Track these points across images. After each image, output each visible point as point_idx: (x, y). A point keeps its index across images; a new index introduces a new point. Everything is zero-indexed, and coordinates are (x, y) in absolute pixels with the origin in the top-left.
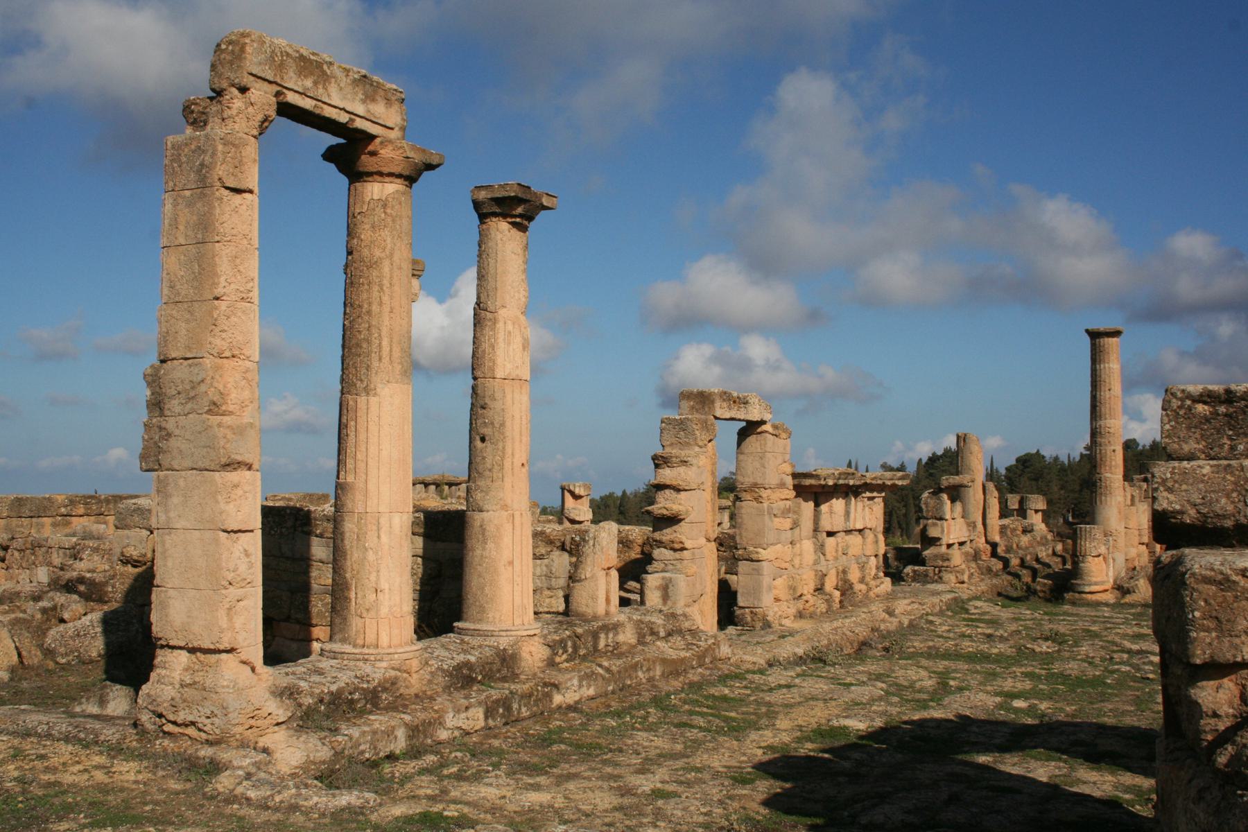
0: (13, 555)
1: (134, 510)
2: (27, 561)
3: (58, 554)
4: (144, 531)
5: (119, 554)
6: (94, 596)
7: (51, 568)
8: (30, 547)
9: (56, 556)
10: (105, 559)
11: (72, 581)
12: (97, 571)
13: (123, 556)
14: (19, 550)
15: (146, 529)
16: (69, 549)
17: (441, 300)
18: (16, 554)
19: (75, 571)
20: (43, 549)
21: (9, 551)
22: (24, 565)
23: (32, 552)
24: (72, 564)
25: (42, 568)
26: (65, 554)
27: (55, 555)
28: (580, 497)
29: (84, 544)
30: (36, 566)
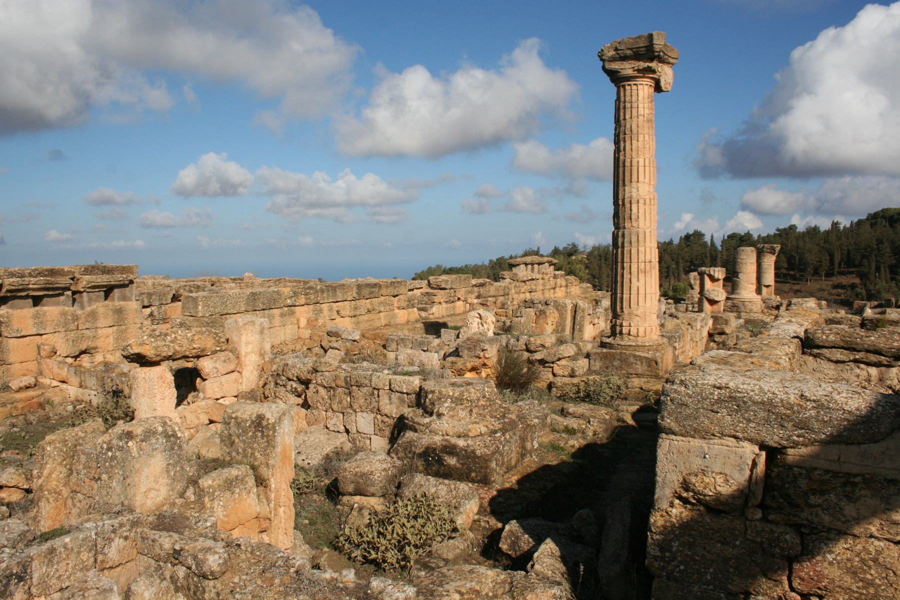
0: (317, 391)
1: (720, 401)
2: (340, 402)
3: (390, 399)
4: (746, 444)
5: (677, 486)
6: (473, 474)
7: (379, 417)
8: (343, 384)
9: (387, 401)
10: (474, 415)
11: (435, 449)
12: (471, 434)
13: (687, 489)
14: (325, 387)
15: (751, 440)
16: (408, 394)
17: (655, 91)
18: (322, 391)
19: (436, 434)
20: (364, 390)
21: (311, 386)
22: (335, 407)
23: (347, 391)
24: (430, 423)
25: (365, 414)
26: (402, 401)
27: (384, 401)
28: (718, 280)
29: (440, 392)
30: (355, 411)
